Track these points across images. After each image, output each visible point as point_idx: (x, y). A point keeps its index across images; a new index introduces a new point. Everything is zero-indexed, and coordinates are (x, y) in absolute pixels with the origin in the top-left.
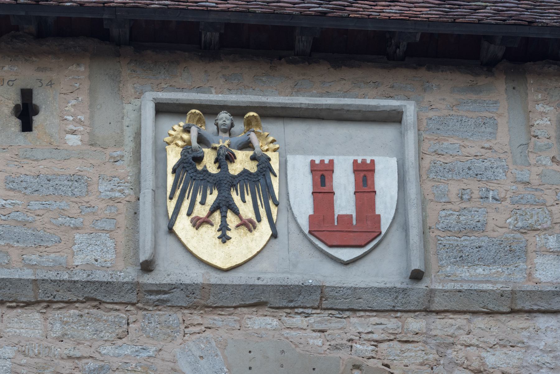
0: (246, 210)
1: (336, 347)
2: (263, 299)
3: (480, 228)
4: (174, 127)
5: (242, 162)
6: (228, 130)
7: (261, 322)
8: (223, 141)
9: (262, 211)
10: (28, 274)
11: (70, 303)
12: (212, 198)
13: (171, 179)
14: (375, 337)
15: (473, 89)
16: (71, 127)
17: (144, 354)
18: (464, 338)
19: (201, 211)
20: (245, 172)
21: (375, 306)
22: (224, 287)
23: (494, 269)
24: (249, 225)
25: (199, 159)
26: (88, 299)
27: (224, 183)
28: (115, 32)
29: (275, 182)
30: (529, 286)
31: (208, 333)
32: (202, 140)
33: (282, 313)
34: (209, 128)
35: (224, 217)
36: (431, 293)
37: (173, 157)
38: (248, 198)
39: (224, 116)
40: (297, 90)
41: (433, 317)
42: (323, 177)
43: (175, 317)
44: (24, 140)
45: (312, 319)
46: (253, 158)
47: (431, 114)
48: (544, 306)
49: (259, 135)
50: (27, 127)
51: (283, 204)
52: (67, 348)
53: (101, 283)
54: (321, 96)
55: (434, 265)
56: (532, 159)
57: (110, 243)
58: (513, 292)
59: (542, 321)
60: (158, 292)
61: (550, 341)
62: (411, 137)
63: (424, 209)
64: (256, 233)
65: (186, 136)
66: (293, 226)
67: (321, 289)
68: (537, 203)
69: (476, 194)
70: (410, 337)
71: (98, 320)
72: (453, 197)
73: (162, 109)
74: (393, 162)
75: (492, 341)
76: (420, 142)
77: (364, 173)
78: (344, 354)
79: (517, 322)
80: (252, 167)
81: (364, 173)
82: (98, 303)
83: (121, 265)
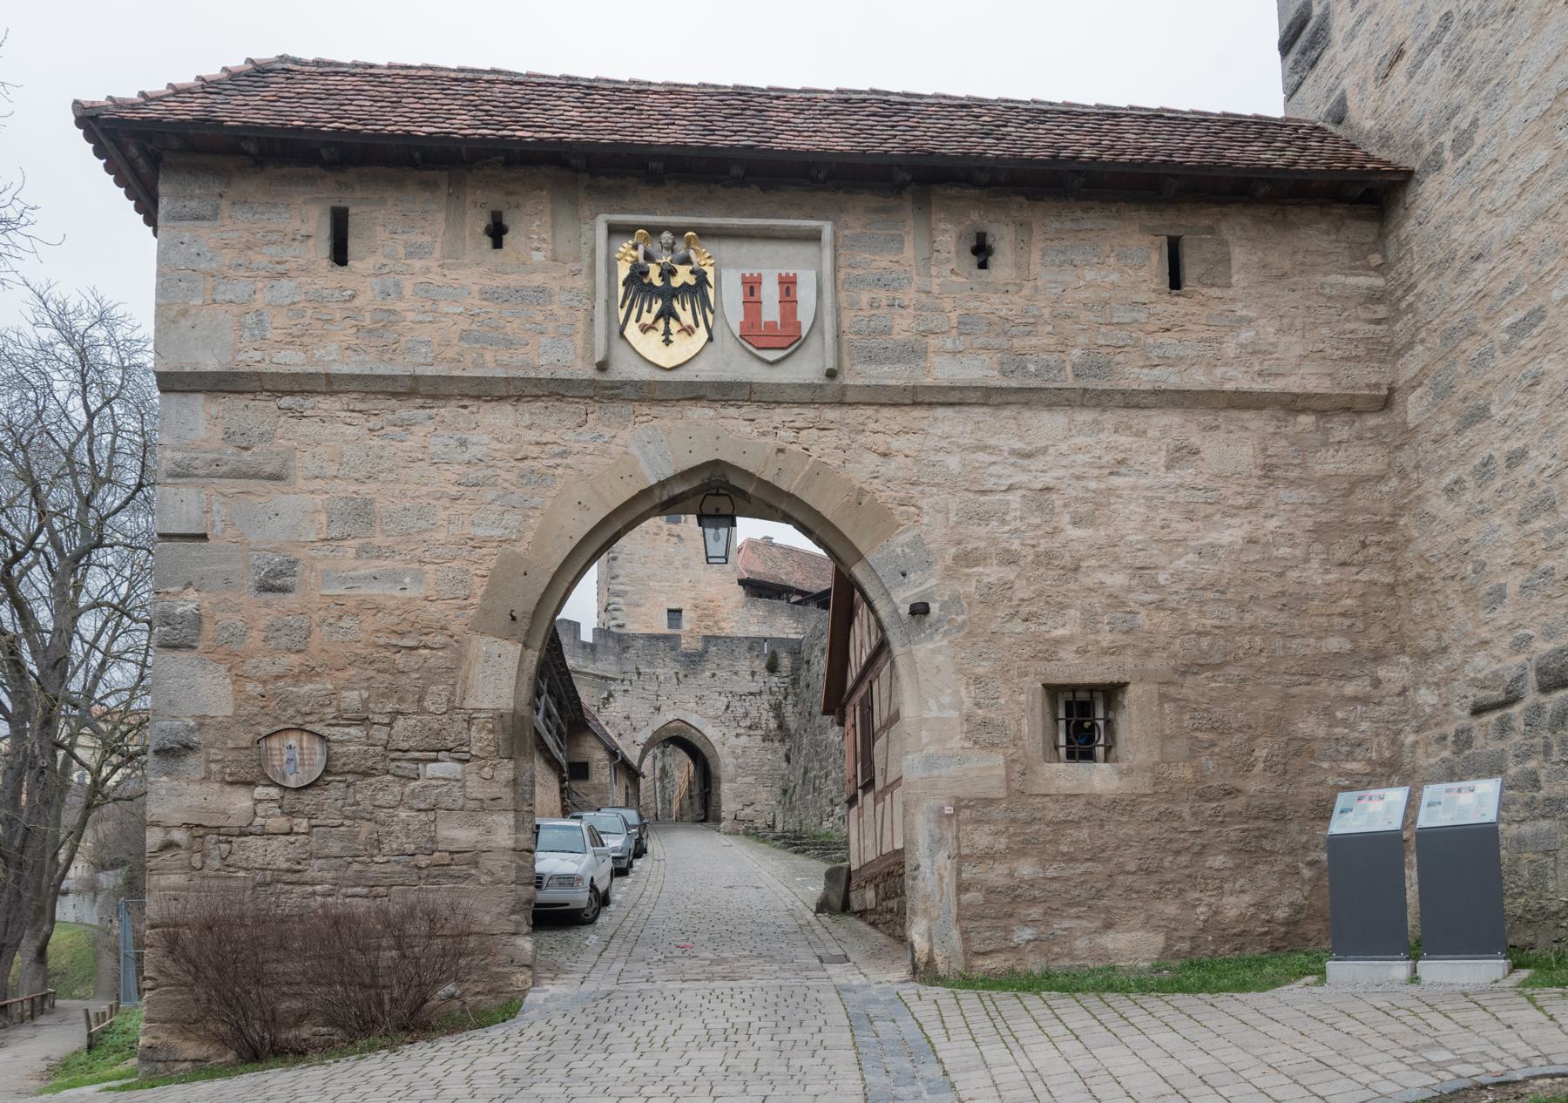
0: (686, 317)
1: (764, 434)
2: (701, 393)
3: (887, 331)
4: (624, 246)
5: (683, 276)
6: (671, 249)
7: (701, 413)
8: (665, 259)
9: (700, 318)
10: (500, 373)
11: (537, 397)
12: (657, 307)
13: (621, 290)
14: (797, 425)
15: (883, 210)
16: (536, 244)
17: (600, 441)
18: (872, 426)
19: (648, 318)
20: (685, 285)
21: (796, 398)
22: (668, 383)
23: (898, 367)
24: (689, 331)
25: (646, 273)
26: (551, 394)
27: (668, 294)
28: (573, 162)
29: (711, 293)
30: (929, 381)
31: (655, 422)
32: (648, 257)
33: (718, 405)
34: (654, 247)
35: (667, 323)
36: (845, 387)
37: (623, 271)
38: (688, 307)
39: (666, 236)
40: (731, 212)
41: (845, 409)
42: (752, 288)
43: (627, 409)
44: (495, 257)
45: (743, 410)
46: (692, 272)
47: (846, 232)
48: (942, 399)
49: (697, 252)
50: (498, 244)
51: (718, 312)
52: (533, 435)
53: (563, 380)
54: (751, 217)
55: (847, 364)
56: (934, 271)
57: (569, 345)
58: (914, 387)
59: (940, 412)
60: (612, 388)
61: (947, 429)
62: (827, 253)
63: (838, 316)
64: (695, 337)
65: (634, 253)
66: (726, 330)
67: (750, 384)
68: (935, 309)
69: (884, 302)
70: (826, 425)
71: (561, 411)
72: (864, 304)
73: (614, 230)
74: (812, 275)
75: (897, 428)
76: (836, 257)
77: (788, 285)
78: (770, 440)
79: (918, 413)
80: (692, 281)
81: (788, 285)
82: (561, 397)
83: (579, 364)
